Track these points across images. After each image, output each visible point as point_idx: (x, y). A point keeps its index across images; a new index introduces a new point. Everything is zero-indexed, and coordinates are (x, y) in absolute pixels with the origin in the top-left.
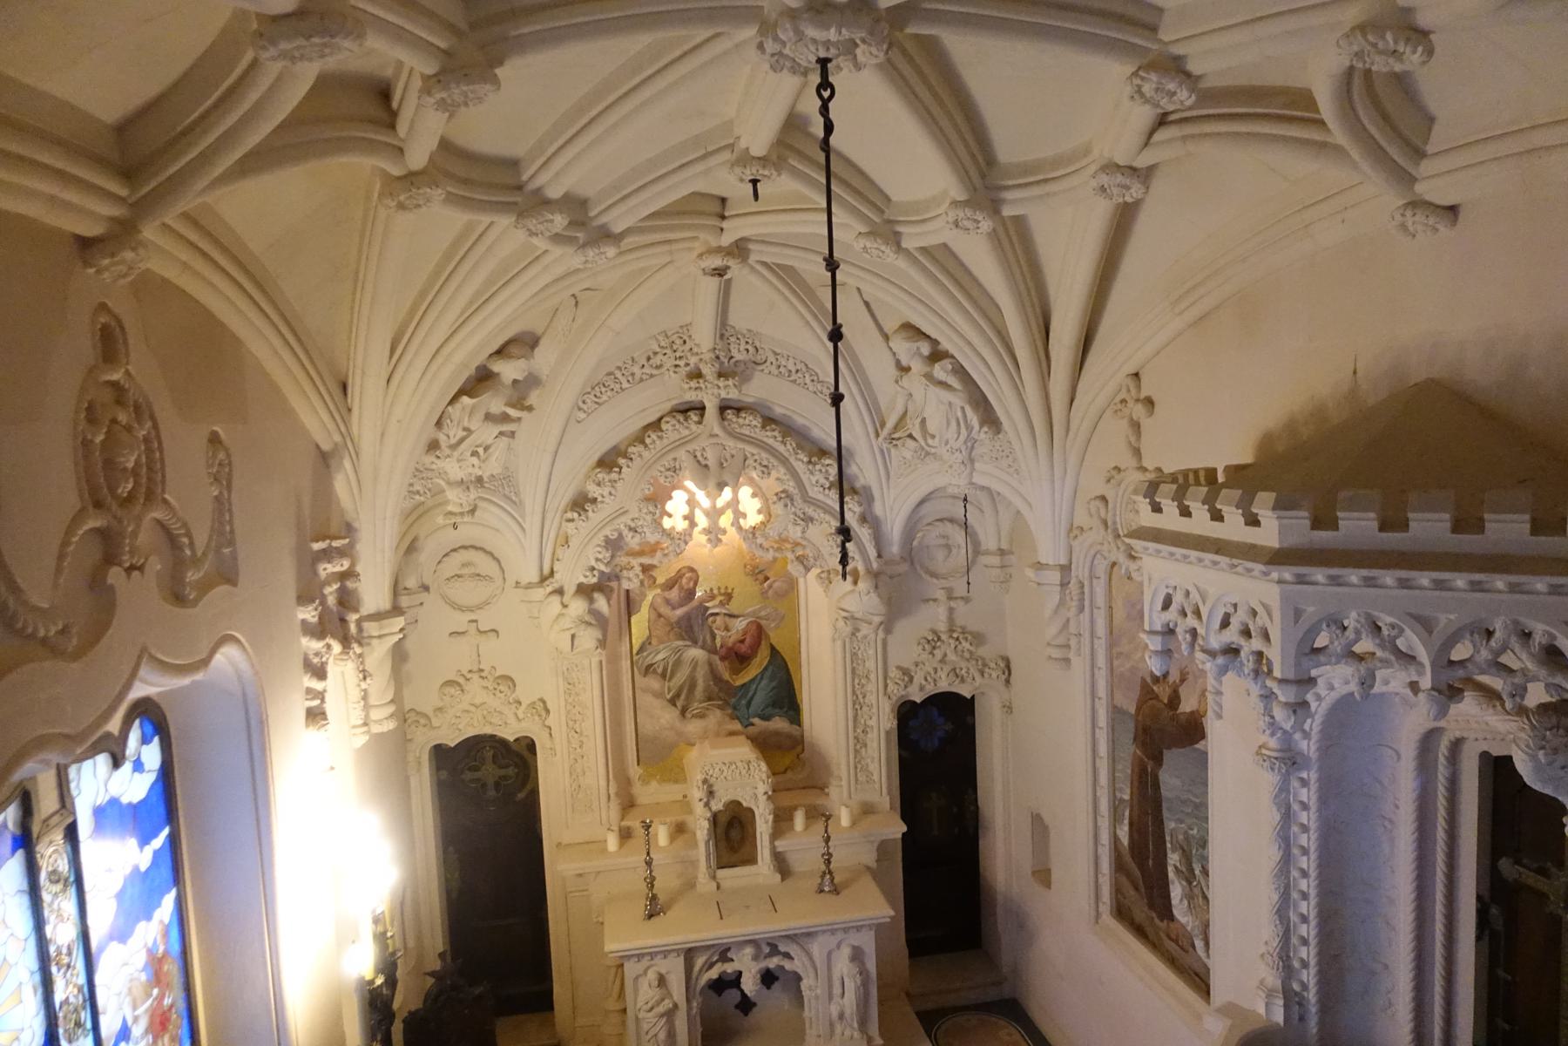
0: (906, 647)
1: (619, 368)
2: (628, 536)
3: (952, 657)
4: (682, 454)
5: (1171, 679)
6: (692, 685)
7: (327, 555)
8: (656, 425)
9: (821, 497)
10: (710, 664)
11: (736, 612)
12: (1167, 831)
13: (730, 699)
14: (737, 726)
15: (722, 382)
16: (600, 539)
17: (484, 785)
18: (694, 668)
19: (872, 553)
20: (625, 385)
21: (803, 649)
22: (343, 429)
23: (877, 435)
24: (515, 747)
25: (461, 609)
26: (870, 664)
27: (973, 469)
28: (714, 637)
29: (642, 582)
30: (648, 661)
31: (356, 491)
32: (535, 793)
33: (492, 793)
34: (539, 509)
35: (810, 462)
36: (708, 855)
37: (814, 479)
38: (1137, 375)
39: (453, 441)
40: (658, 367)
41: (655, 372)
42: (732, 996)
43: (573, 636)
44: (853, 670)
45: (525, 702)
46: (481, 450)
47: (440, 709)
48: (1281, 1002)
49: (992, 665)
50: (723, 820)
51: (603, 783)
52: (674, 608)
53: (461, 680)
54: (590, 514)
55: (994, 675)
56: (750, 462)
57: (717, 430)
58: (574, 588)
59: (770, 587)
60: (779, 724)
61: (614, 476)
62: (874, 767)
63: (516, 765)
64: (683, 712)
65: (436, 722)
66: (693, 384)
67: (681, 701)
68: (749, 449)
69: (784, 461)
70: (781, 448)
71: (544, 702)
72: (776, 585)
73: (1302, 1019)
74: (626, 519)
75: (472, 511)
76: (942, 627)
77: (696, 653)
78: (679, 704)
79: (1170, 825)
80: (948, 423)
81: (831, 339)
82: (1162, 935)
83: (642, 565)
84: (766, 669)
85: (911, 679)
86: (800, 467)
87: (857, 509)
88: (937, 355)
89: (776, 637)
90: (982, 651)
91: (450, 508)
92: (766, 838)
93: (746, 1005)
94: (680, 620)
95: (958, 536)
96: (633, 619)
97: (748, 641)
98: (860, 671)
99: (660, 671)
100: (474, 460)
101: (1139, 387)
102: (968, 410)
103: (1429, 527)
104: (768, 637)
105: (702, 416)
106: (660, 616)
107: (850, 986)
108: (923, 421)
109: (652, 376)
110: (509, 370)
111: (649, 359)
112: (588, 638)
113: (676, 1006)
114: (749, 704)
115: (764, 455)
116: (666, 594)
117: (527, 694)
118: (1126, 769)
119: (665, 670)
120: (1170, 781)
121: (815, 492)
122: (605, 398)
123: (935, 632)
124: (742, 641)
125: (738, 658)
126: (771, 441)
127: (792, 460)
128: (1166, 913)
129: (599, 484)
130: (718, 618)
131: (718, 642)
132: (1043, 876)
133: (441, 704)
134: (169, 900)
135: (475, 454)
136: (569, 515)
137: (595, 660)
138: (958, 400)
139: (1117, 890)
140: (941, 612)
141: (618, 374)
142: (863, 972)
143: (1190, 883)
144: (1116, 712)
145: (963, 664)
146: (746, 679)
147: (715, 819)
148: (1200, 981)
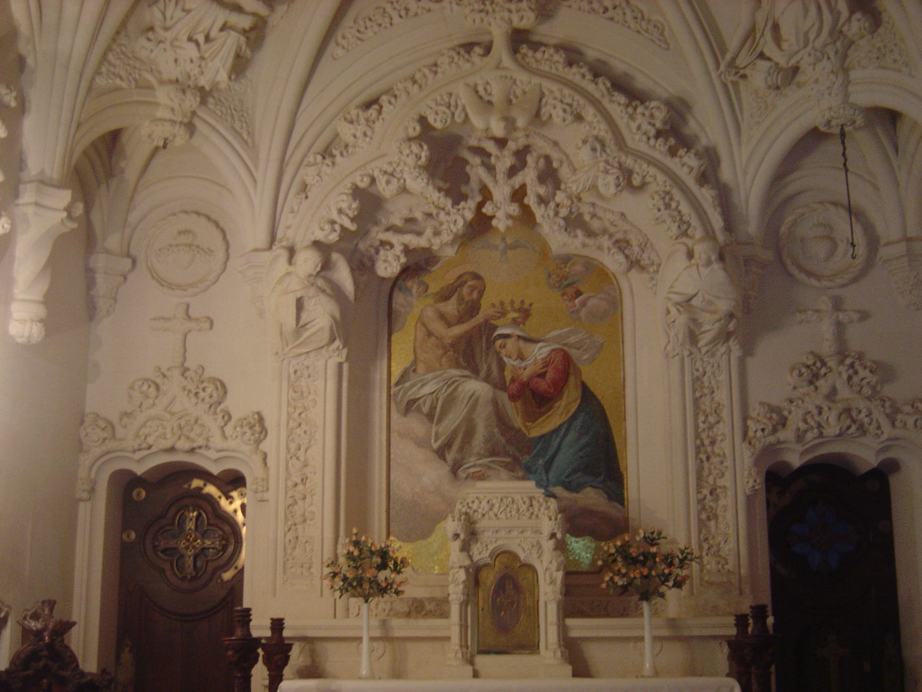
0: (773, 373)
3: (844, 392)
6: (469, 433)
9: (643, 147)
10: (495, 403)
11: (533, 335)
13: (520, 454)
15: (513, 7)
18: (473, 408)
19: (717, 222)
20: (396, 20)
21: (629, 401)
25: (171, 286)
26: (722, 396)
27: (847, 83)
28: (502, 366)
30: (413, 393)
31: (36, 26)
34: (275, 154)
36: (463, 626)
37: (634, 126)
43: (300, 305)
44: (696, 401)
46: (201, 38)
47: (126, 414)
49: (908, 409)
50: (489, 579)
51: (329, 534)
52: (449, 325)
53: (159, 381)
54: (339, 159)
55: (910, 421)
56: (548, 99)
57: (507, 61)
58: (307, 242)
59: (584, 304)
60: (591, 497)
61: (373, 112)
62: (727, 549)
64: (455, 470)
65: (120, 432)
67: (452, 452)
68: (547, 85)
70: (591, 87)
71: (261, 420)
72: (592, 302)
76: (827, 348)
78: (451, 456)
80: (806, 11)
84: (574, 417)
85: (783, 422)
89: (591, 375)
90: (888, 390)
91: (161, 113)
92: (552, 609)
95: (841, 223)
96: (393, 338)
97: (550, 375)
98: (706, 404)
99: (426, 409)
100: (191, 51)
104: (578, 372)
106: (430, 334)
108: (776, 27)
114: (548, 467)
115: (567, 91)
119: (433, 408)
121: (636, 141)
122: (370, 33)
124: (542, 375)
125: (535, 397)
126: (577, 79)
127: (605, 102)
129: (351, 122)
130: (510, 342)
131: (508, 375)
140: (826, 329)
141: (389, 8)
145: (863, 405)
147: (475, 574)
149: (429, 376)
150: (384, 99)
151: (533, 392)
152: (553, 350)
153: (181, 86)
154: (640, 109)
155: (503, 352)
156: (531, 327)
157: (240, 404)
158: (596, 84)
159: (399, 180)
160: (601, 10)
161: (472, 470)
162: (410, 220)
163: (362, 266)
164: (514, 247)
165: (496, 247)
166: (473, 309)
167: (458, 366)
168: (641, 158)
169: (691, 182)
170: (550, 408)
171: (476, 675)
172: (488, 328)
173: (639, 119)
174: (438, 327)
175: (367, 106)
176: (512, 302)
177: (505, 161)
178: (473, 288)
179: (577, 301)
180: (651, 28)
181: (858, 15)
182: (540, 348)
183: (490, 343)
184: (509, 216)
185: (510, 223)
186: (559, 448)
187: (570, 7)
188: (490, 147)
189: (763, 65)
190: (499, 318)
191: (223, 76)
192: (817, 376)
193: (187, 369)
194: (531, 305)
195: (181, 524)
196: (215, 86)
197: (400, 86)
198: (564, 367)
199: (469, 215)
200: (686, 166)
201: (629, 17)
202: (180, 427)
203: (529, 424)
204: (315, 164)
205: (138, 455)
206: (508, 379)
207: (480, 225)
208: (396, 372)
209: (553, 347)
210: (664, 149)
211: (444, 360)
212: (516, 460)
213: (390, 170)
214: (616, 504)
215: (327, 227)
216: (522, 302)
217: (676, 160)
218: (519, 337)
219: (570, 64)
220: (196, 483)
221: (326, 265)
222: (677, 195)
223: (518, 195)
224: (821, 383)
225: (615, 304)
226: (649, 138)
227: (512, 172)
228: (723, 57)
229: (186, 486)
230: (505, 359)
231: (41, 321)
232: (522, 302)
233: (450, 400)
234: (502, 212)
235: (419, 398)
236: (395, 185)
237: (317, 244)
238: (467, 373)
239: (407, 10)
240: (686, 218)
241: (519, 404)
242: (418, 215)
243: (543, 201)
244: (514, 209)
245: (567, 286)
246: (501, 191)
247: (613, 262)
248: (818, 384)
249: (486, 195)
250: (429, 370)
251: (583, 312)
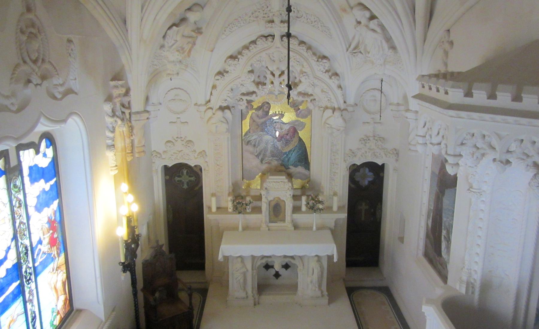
1: (240, 17)
4: (263, 54)
7: (116, 87)
8: (254, 42)
12: (443, 221)
14: (283, 168)
16: (229, 88)
17: (183, 183)
22: (124, 38)
23: (347, 50)
24: (195, 169)
29: (247, 107)
30: (248, 139)
32: (202, 187)
33: (185, 186)
35: (318, 61)
38: (449, 30)
39: (170, 45)
42: (272, 272)
45: (198, 152)
47: (165, 152)
48: (465, 286)
49: (391, 152)
50: (273, 204)
53: (174, 141)
54: (225, 77)
59: (300, 112)
60: (300, 169)
61: (236, 62)
63: (196, 177)
64: (262, 161)
65: (163, 156)
66: (270, 25)
69: (306, 60)
72: (303, 112)
73: (473, 293)
75: (178, 74)
77: (268, 137)
79: (444, 219)
81: (287, 11)
82: (438, 263)
84: (296, 146)
87: (337, 82)
88: (373, 17)
89: (302, 134)
91: (168, 72)
93: (277, 275)
94: (263, 123)
99: (253, 144)
101: (449, 36)
103: (504, 99)
105: (273, 39)
106: (254, 121)
107: (316, 271)
109: (254, 21)
110: (192, 17)
111: (253, 14)
112: (224, 127)
113: (247, 270)
115: (298, 57)
118: (433, 197)
120: (446, 201)
123: (367, 137)
124: (287, 134)
126: (302, 51)
128: (439, 254)
132: (401, 239)
133: (166, 150)
134: (56, 202)
136: (217, 77)
139: (426, 246)
141: (240, 20)
142: (321, 267)
143: (448, 242)
144: (433, 173)
146: (289, 149)
148: (444, 278)
149: (254, 134)
156: (285, 120)
168: (320, 80)
171: (269, 230)
178: (267, 107)
180: (327, 31)
181: (391, 51)
187: (300, 21)
192: (366, 143)
193: (181, 138)
195: (183, 173)
198: (294, 131)
200: (333, 83)
201: (319, 23)
204: (218, 80)
206: (277, 134)
210: (328, 77)
213: (242, 83)
222: (330, 93)
224: (367, 144)
227: (280, 76)
228: (350, 46)
232: (282, 112)
240: (332, 101)
246: (276, 83)
248: (367, 144)
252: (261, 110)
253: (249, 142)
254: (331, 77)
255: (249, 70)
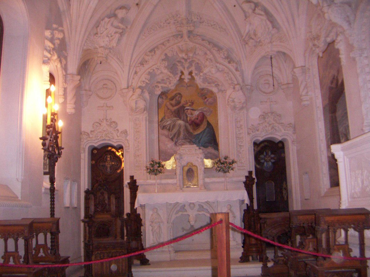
2: (156, 70)
5: (335, 77)
9: (222, 61)
11: (195, 109)
13: (191, 139)
16: (147, 71)
25: (102, 98)
30: (165, 124)
39: (102, 32)
40: (169, 23)
41: (168, 25)
45: (120, 131)
46: (110, 36)
47: (91, 131)
50: (186, 169)
54: (144, 65)
57: (187, 39)
60: (210, 150)
61: (153, 53)
64: (176, 143)
65: (91, 136)
68: (197, 46)
69: (209, 50)
72: (209, 100)
74: (156, 66)
77: (181, 122)
78: (175, 139)
83: (162, 86)
84: (205, 129)
86: (215, 52)
87: (235, 65)
96: (159, 110)
97: (199, 118)
99: (168, 128)
100: (107, 39)
102: (267, 21)
104: (206, 118)
106: (168, 109)
110: (121, 14)
114: (199, 142)
116: (171, 102)
117: (121, 127)
119: (170, 127)
124: (197, 119)
125: (196, 124)
127: (212, 49)
130: (189, 111)
131: (188, 119)
133: (93, 130)
135: (107, 36)
137: (145, 116)
138: (264, 18)
144: (324, 108)
145: (277, 125)
149: (169, 119)
150: (156, 49)
151: (195, 123)
152: (200, 112)
153: (105, 48)
154: (221, 52)
155: (187, 113)
156: (194, 107)
157: (121, 127)
158: (210, 45)
159: (160, 70)
160: (211, 26)
161: (180, 143)
162: (163, 80)
163: (151, 93)
164: (190, 86)
165: (185, 87)
166: (179, 103)
167: (176, 117)
169: (234, 70)
170: (199, 128)
172: (183, 107)
173: (221, 54)
174: (171, 107)
175: (151, 51)
176: (189, 101)
177: (186, 65)
178: (179, 97)
179: (206, 100)
182: (197, 112)
183: (184, 111)
184: (189, 79)
185: (189, 80)
186: (202, 137)
188: (183, 61)
189: (251, 41)
190: (186, 104)
191: (115, 45)
193: (107, 120)
194: (194, 101)
195: (106, 159)
196: (113, 47)
197: (159, 46)
198: (203, 117)
199: (178, 79)
202: (106, 134)
203: (194, 131)
204: (138, 66)
205: (96, 141)
207: (181, 80)
208: (160, 120)
209: (201, 111)
211: (172, 116)
212: (191, 140)
213: (158, 68)
214: (217, 151)
215: (142, 83)
216: (192, 100)
217: (230, 64)
218: (191, 109)
219: (203, 40)
220: (110, 148)
221: (142, 92)
223: (190, 73)
225: (215, 100)
226: (223, 59)
227: (188, 68)
229: (107, 149)
230: (188, 115)
231: (74, 108)
232: (192, 100)
233: (174, 126)
234: (186, 77)
235: (166, 125)
236: (159, 72)
237: (140, 87)
238: (178, 119)
239: (161, 26)
240: (232, 79)
241: (191, 126)
242: (165, 79)
243: (196, 74)
244: (190, 77)
245: (203, 96)
246: (186, 73)
247: (215, 90)
249: (182, 73)
250: (169, 118)
251: (207, 103)
252: (174, 100)
253: (164, 127)
254: (229, 62)
255: (163, 58)
